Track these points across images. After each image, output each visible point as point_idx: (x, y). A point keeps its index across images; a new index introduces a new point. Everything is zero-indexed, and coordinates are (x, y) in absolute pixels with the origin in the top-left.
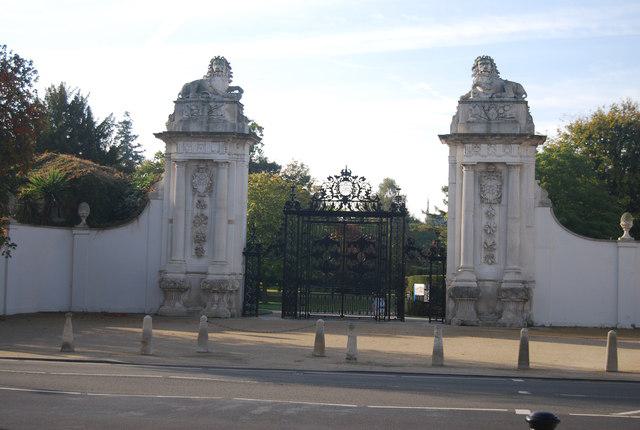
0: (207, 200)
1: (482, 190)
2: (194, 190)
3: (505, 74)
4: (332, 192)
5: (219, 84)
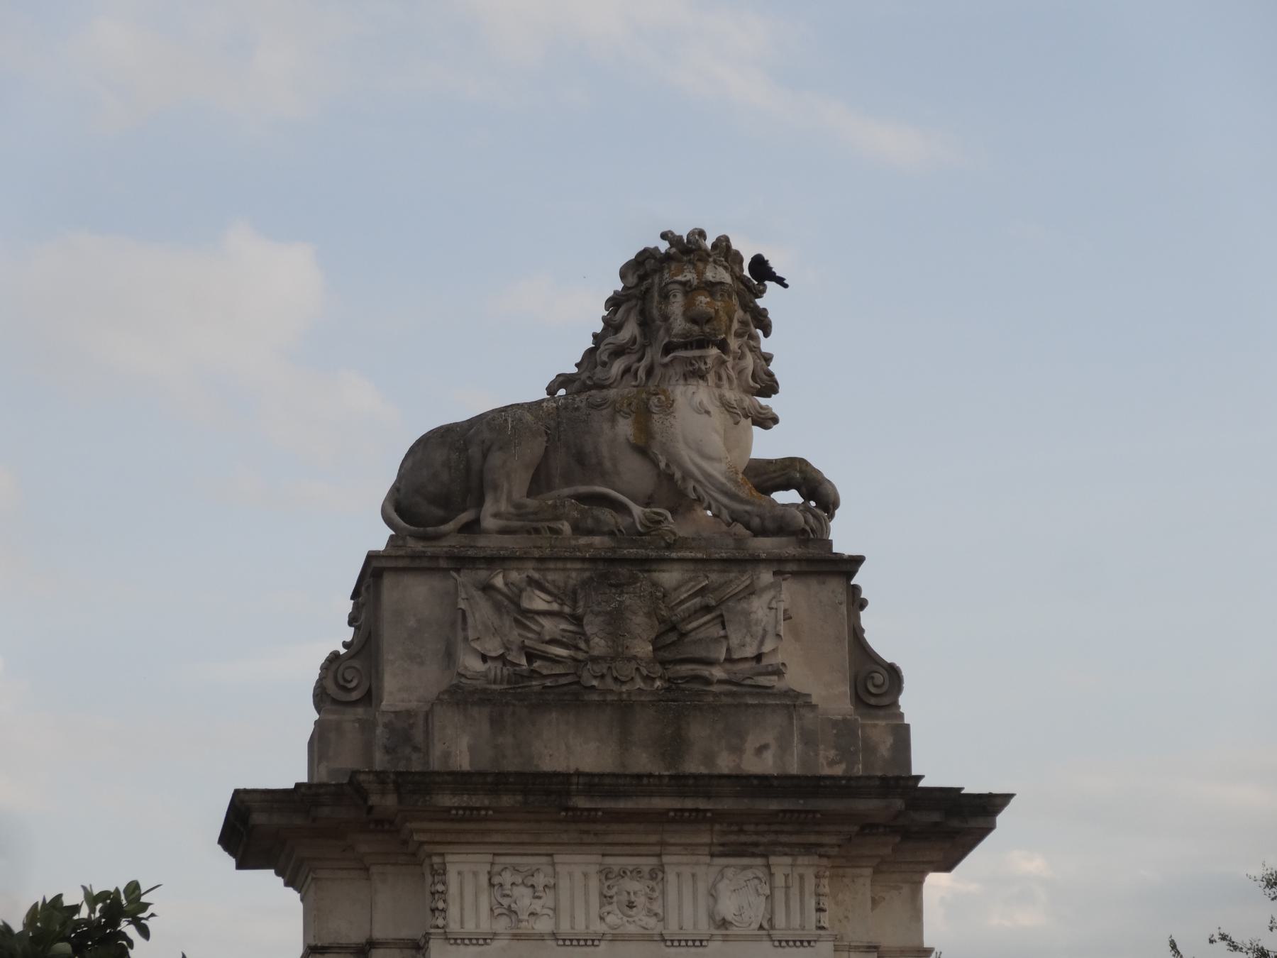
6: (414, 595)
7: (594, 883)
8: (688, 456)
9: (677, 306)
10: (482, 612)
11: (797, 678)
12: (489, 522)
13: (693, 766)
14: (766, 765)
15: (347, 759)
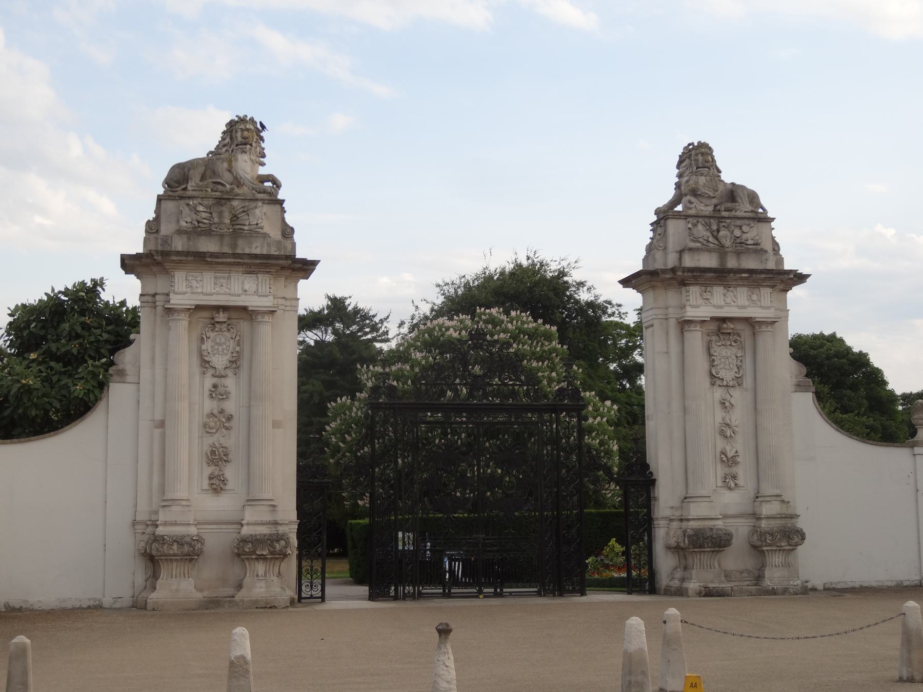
0: (230, 383)
1: (712, 363)
2: (205, 363)
3: (731, 172)
6: (169, 205)
7: (213, 280)
8: (241, 173)
9: (239, 134)
10: (186, 210)
11: (267, 229)
12: (189, 188)
13: (239, 251)
14: (257, 251)
15: (152, 247)
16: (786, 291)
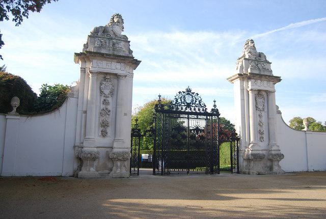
0: (110, 99)
1: (256, 103)
2: (101, 92)
4: (181, 100)
5: (117, 29)
16: (274, 84)
